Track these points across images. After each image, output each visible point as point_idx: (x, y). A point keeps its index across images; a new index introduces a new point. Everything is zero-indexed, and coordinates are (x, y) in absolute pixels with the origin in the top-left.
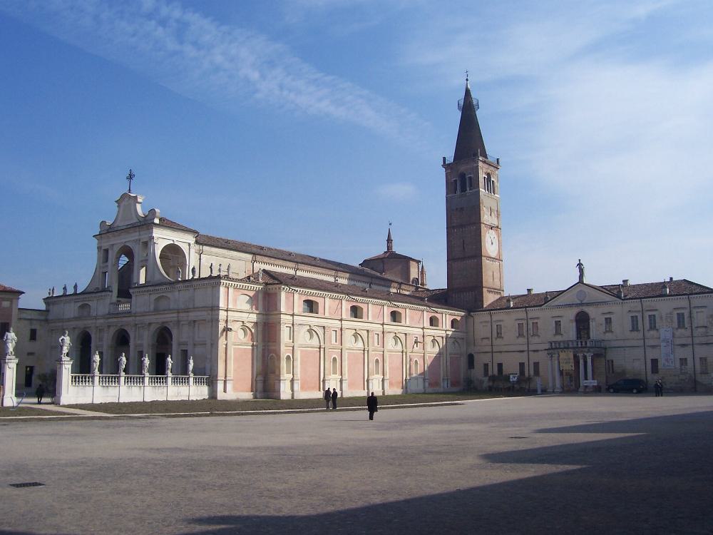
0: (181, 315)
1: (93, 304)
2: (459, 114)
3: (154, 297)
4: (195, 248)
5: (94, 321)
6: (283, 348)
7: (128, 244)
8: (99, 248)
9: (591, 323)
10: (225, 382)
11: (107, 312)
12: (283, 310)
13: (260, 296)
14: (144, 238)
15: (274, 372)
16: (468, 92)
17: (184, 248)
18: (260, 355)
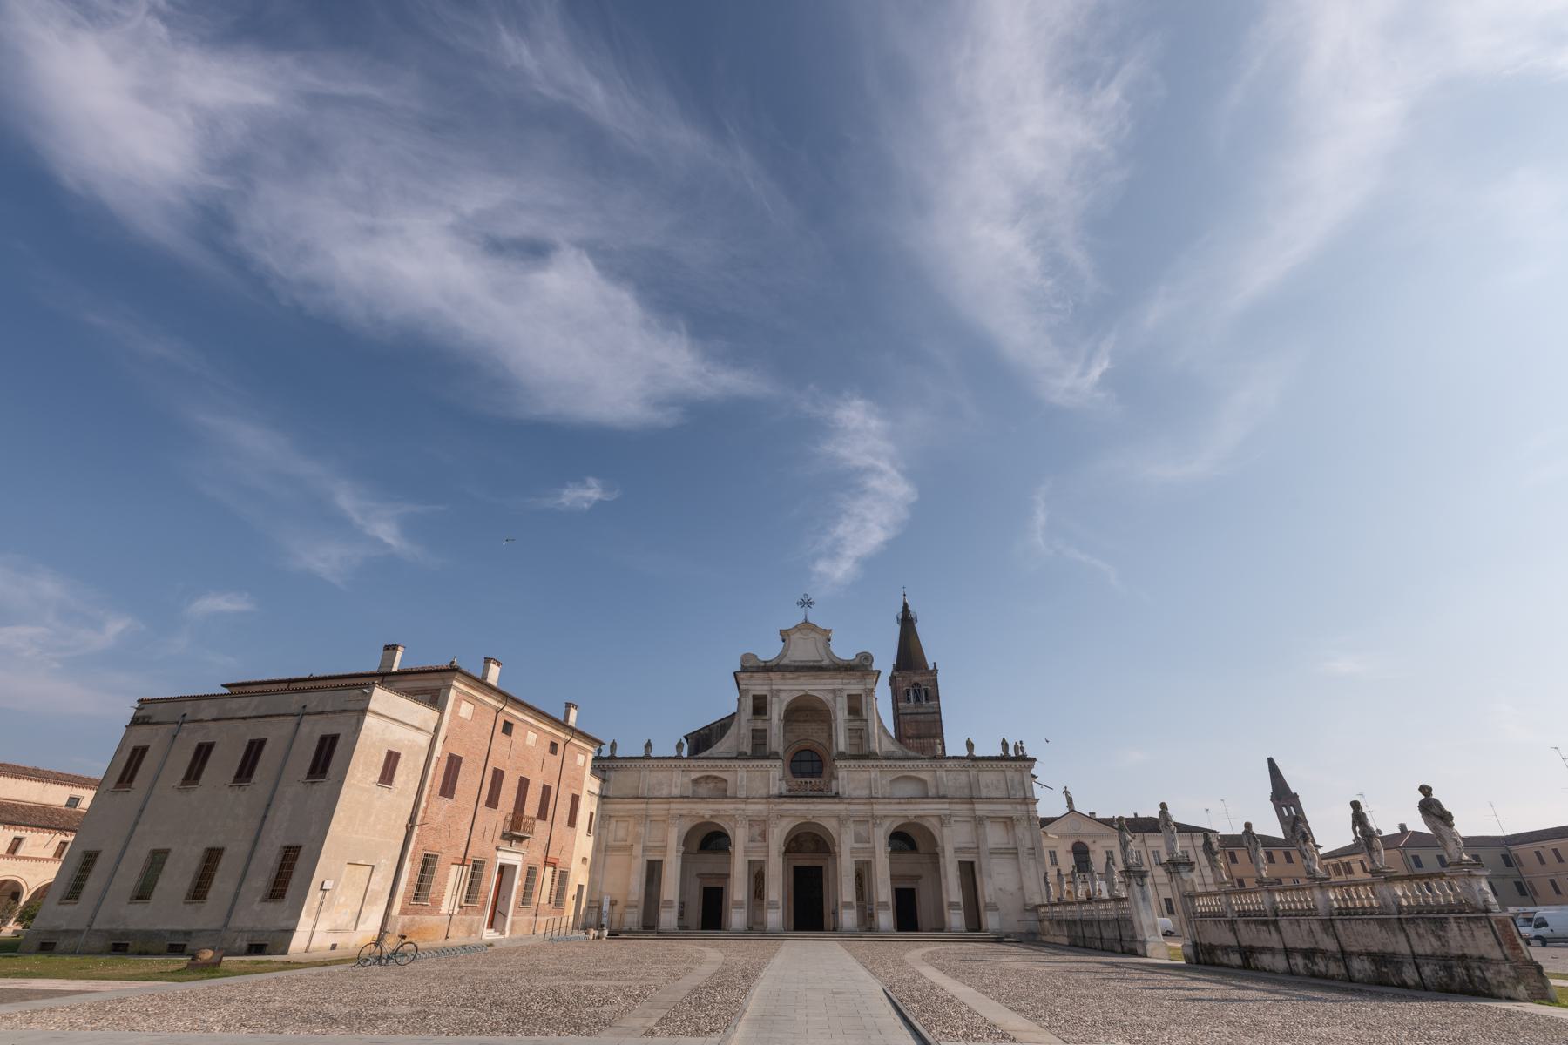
2: (898, 628)
3: (890, 777)
5: (743, 806)
9: (1091, 856)
11: (774, 791)
14: (855, 688)
16: (906, 606)
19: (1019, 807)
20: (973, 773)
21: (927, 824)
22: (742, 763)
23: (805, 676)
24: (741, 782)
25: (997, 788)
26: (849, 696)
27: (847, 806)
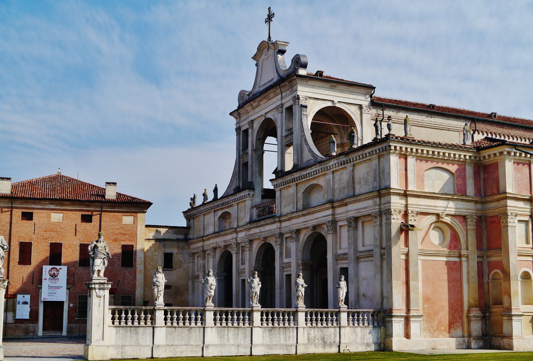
0: (339, 210)
1: (232, 211)
3: (302, 188)
4: (370, 114)
5: (234, 235)
6: (513, 258)
7: (269, 116)
8: (238, 129)
10: (407, 320)
11: (248, 220)
12: (510, 189)
13: (469, 171)
15: (501, 303)
17: (353, 112)
18: (474, 273)
19: (378, 199)
20: (349, 167)
22: (233, 198)
23: (262, 100)
24: (235, 214)
26: (287, 109)
27: (278, 224)
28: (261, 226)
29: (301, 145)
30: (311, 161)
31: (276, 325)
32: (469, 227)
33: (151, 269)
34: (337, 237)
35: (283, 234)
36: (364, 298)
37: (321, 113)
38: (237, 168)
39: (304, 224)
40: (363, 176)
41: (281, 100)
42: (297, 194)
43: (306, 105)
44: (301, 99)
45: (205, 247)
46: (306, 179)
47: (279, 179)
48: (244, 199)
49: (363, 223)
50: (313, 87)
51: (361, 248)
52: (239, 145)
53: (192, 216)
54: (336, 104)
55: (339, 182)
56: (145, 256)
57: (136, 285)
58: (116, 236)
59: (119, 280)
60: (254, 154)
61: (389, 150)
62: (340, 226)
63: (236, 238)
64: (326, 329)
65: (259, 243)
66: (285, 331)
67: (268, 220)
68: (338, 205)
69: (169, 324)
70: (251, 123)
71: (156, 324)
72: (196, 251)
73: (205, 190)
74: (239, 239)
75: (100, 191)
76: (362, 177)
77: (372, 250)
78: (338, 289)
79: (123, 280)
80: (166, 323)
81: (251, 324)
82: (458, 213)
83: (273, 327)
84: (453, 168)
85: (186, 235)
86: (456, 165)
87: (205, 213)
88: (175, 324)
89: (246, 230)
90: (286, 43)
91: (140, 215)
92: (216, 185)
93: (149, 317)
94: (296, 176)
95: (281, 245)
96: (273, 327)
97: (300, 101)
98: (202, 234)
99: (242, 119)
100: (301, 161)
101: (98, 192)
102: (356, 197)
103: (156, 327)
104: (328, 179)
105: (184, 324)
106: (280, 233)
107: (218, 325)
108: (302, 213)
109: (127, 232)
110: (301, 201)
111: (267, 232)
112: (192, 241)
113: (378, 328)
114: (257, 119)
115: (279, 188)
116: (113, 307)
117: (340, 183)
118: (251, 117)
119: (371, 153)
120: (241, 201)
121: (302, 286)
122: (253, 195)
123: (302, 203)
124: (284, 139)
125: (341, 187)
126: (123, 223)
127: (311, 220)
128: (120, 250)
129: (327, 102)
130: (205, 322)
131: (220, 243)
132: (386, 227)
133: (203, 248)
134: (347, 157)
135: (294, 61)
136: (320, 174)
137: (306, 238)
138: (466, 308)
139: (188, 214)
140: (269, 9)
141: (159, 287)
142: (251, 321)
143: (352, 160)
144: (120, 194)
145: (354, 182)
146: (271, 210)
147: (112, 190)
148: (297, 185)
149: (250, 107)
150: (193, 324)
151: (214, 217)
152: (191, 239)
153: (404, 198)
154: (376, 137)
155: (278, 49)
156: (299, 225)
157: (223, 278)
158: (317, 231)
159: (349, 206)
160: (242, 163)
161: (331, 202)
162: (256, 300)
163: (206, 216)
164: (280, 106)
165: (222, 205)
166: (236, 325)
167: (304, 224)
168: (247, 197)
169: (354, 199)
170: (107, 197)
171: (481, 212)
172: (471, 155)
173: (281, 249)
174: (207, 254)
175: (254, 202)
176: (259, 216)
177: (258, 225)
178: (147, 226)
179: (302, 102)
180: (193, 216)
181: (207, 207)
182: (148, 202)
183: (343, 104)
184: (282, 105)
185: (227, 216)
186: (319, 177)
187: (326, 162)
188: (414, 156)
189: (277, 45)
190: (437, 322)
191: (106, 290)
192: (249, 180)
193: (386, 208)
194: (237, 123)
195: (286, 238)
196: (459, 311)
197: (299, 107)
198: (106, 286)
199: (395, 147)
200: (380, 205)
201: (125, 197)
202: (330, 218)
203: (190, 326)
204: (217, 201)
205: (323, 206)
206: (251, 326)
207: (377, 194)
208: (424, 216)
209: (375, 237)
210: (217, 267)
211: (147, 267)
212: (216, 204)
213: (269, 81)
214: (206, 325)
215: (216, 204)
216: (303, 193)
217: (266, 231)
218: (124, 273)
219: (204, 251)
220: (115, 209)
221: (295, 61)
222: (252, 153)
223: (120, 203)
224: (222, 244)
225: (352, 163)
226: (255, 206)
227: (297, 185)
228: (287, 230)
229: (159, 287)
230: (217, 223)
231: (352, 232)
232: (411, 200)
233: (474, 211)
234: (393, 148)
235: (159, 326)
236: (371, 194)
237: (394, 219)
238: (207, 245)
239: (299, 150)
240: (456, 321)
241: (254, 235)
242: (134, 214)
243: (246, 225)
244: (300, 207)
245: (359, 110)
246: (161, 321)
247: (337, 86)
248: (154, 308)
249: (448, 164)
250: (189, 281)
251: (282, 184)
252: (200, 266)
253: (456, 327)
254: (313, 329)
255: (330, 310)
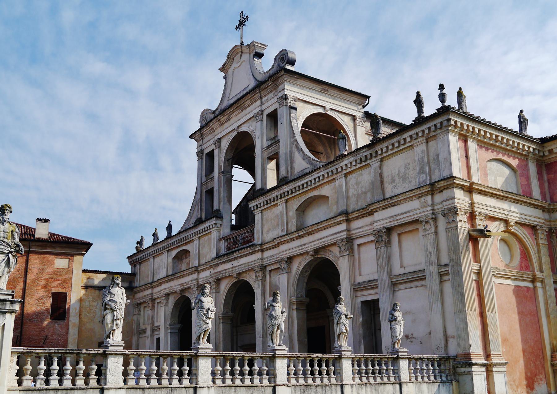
0: (356, 224)
3: (295, 204)
5: (195, 276)
7: (242, 129)
8: (200, 154)
11: (214, 255)
13: (532, 168)
17: (345, 122)
19: (429, 199)
20: (374, 164)
21: (331, 257)
24: (196, 251)
25: (405, 178)
27: (259, 254)
28: (234, 260)
29: (291, 153)
30: (307, 169)
31: (310, 381)
32: (541, 242)
33: (87, 322)
34: (354, 260)
35: (265, 267)
36: (409, 340)
37: (309, 122)
38: (199, 197)
39: (301, 248)
40: (399, 171)
41: (261, 106)
42: (286, 213)
43: (296, 107)
44: (289, 99)
45: (154, 295)
46: (301, 191)
47: (261, 198)
48: (209, 231)
49: (399, 235)
50: (302, 87)
51: (397, 270)
52: (202, 170)
53: (139, 261)
54: (327, 111)
55: (355, 187)
56: (80, 307)
57: (68, 342)
58: (45, 282)
59: (47, 336)
60: (222, 177)
61: (445, 126)
62: (359, 245)
63: (197, 279)
64: (382, 387)
65: (229, 282)
66: (324, 392)
67: (245, 250)
68: (356, 217)
69: (132, 383)
70: (218, 142)
71: (108, 384)
72: (142, 300)
73: (156, 229)
74: (202, 280)
75: (29, 231)
76: (397, 172)
77: (424, 271)
78: (393, 323)
79: (52, 336)
80: (125, 381)
81: (272, 380)
82: (527, 222)
83: (306, 384)
84: (515, 163)
85: (131, 282)
86: (517, 160)
87: (156, 254)
88: (143, 383)
89: (210, 267)
90: (264, 45)
91: (76, 258)
92: (170, 222)
93: (93, 369)
94: (287, 189)
95: (263, 280)
96: (307, 386)
97: (288, 102)
98: (151, 280)
99: (205, 140)
100: (291, 173)
101: (27, 231)
102: (389, 200)
103: (107, 389)
104: (338, 185)
105: (159, 381)
106: (262, 265)
107: (219, 382)
108: (297, 235)
109: (59, 278)
110: (294, 221)
111: (242, 266)
112: (138, 289)
113: (448, 384)
114: (226, 137)
115: (259, 209)
116: (21, 349)
117: (358, 188)
118: (217, 136)
119: (415, 136)
120: (204, 233)
121: (346, 316)
122: (221, 225)
123: (295, 224)
124: (264, 150)
125: (360, 192)
126: (56, 267)
127: (312, 242)
128: (50, 298)
129: (318, 107)
130: (197, 378)
131: (175, 287)
132: (447, 236)
133: (152, 296)
134: (370, 149)
135: (277, 58)
136: (326, 180)
137: (301, 268)
138: (548, 353)
139: (134, 258)
140: (240, 14)
141: (115, 313)
142: (272, 375)
143: (379, 152)
144: (54, 234)
145: (382, 182)
146: (245, 240)
147: (44, 227)
148: (287, 201)
149: (218, 123)
150: (175, 383)
151: (167, 257)
152: (136, 287)
153: (468, 194)
154: (419, 115)
155: (254, 52)
156: (293, 250)
157: (177, 331)
158: (319, 256)
159: (376, 214)
160: (204, 191)
161: (346, 213)
162: (278, 338)
163: (157, 258)
164: (260, 113)
165: (178, 241)
166: (247, 382)
167: (301, 248)
168: (212, 228)
169: (386, 204)
170: (37, 236)
171: (548, 223)
172: (534, 147)
173: (264, 286)
174: (156, 304)
175: (221, 233)
176: (228, 248)
177: (229, 259)
178: (85, 271)
179: (291, 102)
180: (140, 260)
181: (158, 247)
182: (87, 242)
183: (335, 112)
184: (262, 112)
185: (184, 256)
186: (323, 186)
187: (336, 163)
188: (474, 139)
189: (253, 47)
190: (518, 374)
191: (8, 316)
192: (216, 207)
193: (444, 208)
194: (199, 146)
195: (270, 271)
196: (541, 357)
197: (286, 109)
198: (8, 306)
199: (456, 122)
200: (433, 205)
201: (59, 237)
202: (344, 235)
203: (171, 386)
204: (172, 238)
205: (332, 220)
206: (273, 385)
207: (430, 189)
208: (491, 222)
209: (427, 251)
210: (169, 317)
211: (83, 320)
212: (170, 242)
213: (243, 90)
214: (199, 383)
215: (170, 241)
216: (297, 210)
217: (240, 265)
218: (54, 327)
219: (153, 300)
220: (46, 249)
221: (279, 58)
222: (219, 175)
223: (53, 242)
224: (178, 289)
225: (379, 157)
226: (224, 238)
227: (287, 201)
228: (271, 261)
229: (115, 313)
230: (171, 265)
231: (383, 250)
232: (477, 198)
233: (543, 221)
234: (453, 123)
235: (113, 386)
236: (417, 190)
237: (461, 221)
238: (157, 292)
239: (287, 160)
240: (539, 372)
241: (222, 272)
242: (69, 257)
243: (212, 261)
244: (293, 229)
245: (352, 121)
246: (116, 377)
247: (329, 90)
248: (105, 351)
249: (509, 156)
250: (133, 337)
251: (265, 203)
252: (148, 317)
253: (539, 380)
254: (364, 387)
255: (385, 355)
